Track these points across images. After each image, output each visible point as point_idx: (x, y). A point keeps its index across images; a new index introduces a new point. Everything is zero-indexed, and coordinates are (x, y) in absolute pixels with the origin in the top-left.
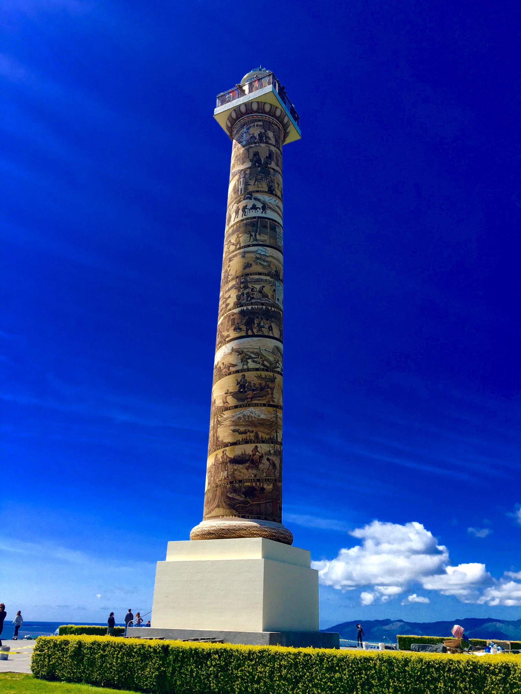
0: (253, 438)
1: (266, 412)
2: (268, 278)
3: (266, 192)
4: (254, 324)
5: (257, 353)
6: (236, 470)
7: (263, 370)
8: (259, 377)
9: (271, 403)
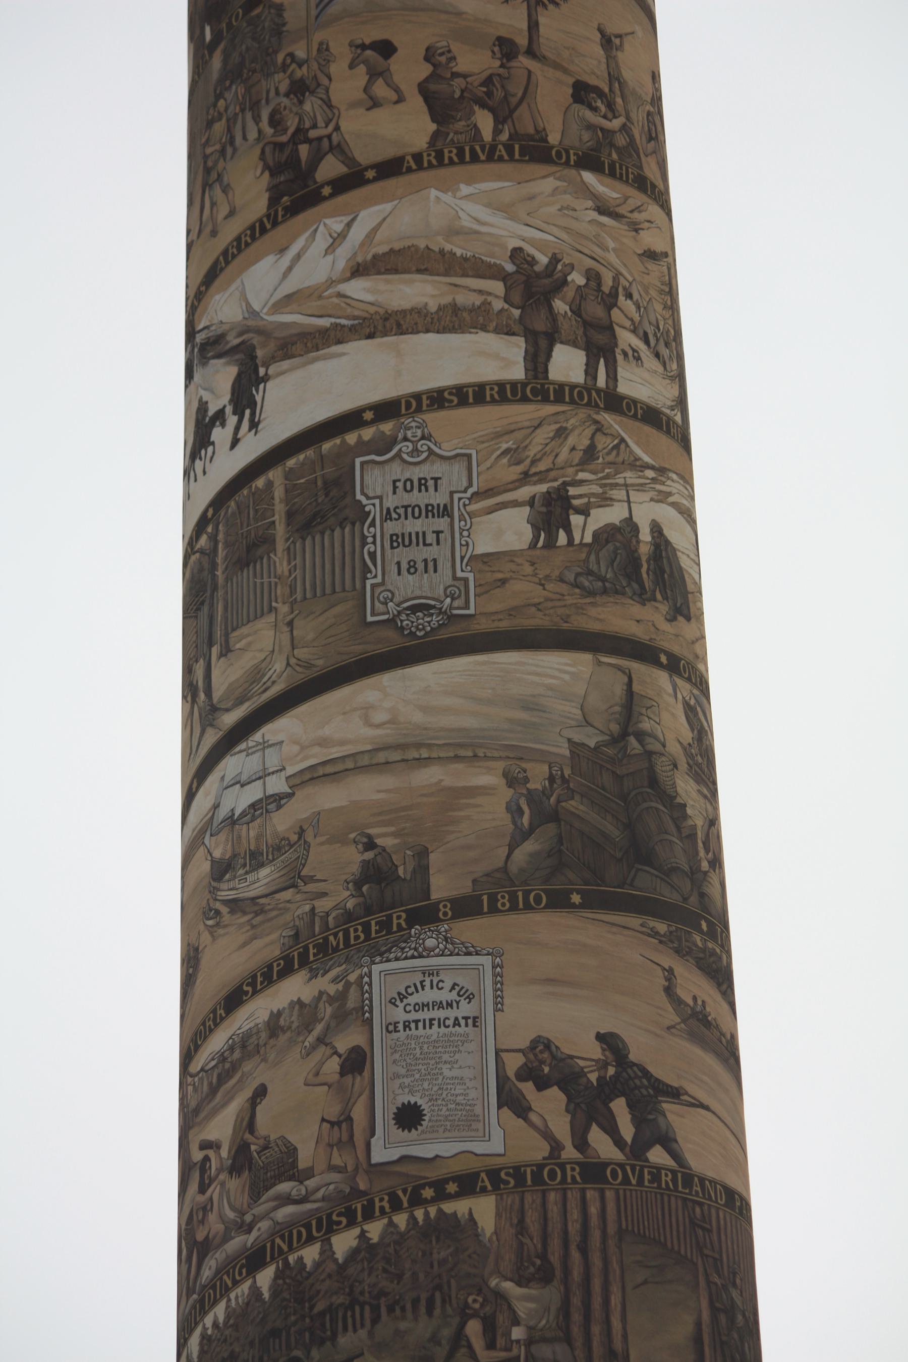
2: (295, 988)
3: (258, 230)
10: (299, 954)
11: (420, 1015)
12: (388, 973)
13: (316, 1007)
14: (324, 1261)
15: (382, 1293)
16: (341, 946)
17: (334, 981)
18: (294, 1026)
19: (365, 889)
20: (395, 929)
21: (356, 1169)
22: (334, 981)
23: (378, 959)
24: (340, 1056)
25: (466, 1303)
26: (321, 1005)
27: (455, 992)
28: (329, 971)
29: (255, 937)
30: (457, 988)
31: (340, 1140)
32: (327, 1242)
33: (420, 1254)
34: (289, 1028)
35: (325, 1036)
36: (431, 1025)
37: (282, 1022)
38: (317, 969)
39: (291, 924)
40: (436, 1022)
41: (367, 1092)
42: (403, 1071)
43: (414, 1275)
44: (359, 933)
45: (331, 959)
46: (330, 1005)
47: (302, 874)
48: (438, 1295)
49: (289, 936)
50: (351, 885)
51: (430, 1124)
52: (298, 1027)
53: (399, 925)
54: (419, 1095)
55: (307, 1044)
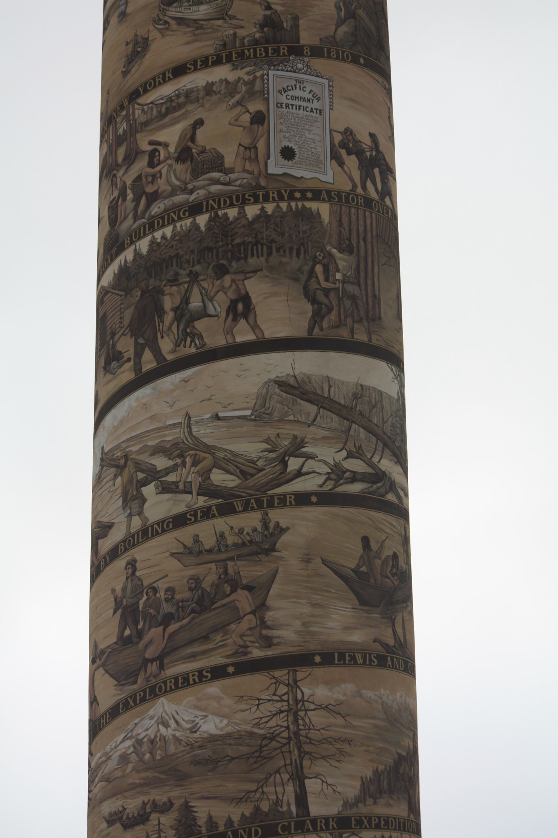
1: (228, 701)
2: (222, 73)
4: (161, 312)
5: (175, 445)
7: (207, 514)
8: (193, 552)
9: (257, 653)
10: (226, 55)
11: (294, 102)
12: (278, 77)
13: (236, 85)
14: (241, 218)
15: (273, 241)
16: (252, 56)
17: (248, 73)
18: (223, 92)
19: (265, 29)
20: (281, 54)
21: (259, 174)
22: (248, 73)
23: (272, 68)
24: (250, 114)
25: (316, 256)
26: (239, 84)
27: (311, 95)
28: (244, 67)
29: (196, 41)
30: (312, 93)
31: (250, 157)
32: (242, 209)
33: (293, 225)
34: (219, 92)
35: (242, 101)
36: (299, 109)
37: (214, 88)
38: (237, 65)
39: (222, 39)
40: (302, 108)
41: (266, 135)
42: (285, 129)
43: (290, 235)
44: (262, 52)
45: (246, 62)
46: (245, 86)
47: (229, 13)
48: (302, 247)
49: (220, 45)
50: (257, 26)
51: (299, 160)
52: (225, 93)
53: (284, 53)
54: (293, 143)
55: (230, 103)
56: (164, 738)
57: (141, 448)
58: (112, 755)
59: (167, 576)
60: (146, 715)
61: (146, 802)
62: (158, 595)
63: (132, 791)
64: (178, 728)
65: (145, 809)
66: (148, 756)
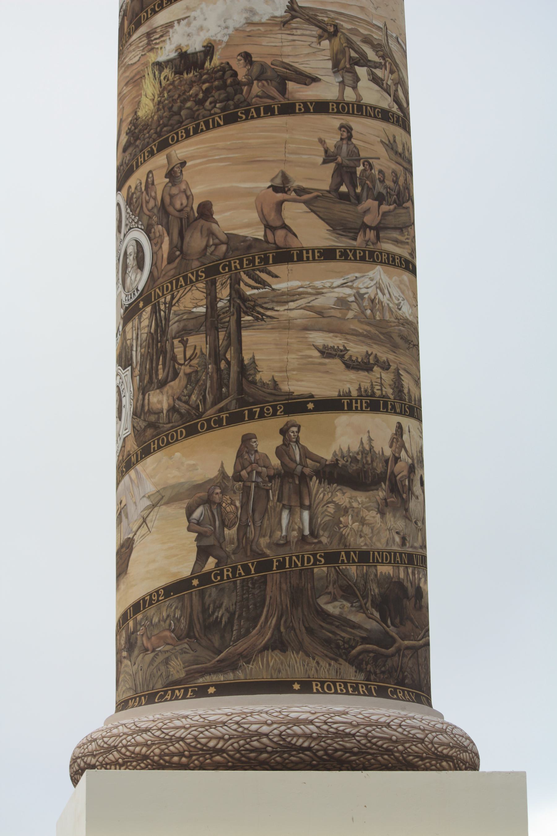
0: (389, 391)
6: (346, 511)
56: (382, 303)
57: (352, 28)
58: (326, 293)
59: (379, 159)
60: (366, 274)
61: (370, 353)
62: (373, 171)
63: (355, 337)
64: (390, 299)
65: (369, 359)
66: (368, 312)
